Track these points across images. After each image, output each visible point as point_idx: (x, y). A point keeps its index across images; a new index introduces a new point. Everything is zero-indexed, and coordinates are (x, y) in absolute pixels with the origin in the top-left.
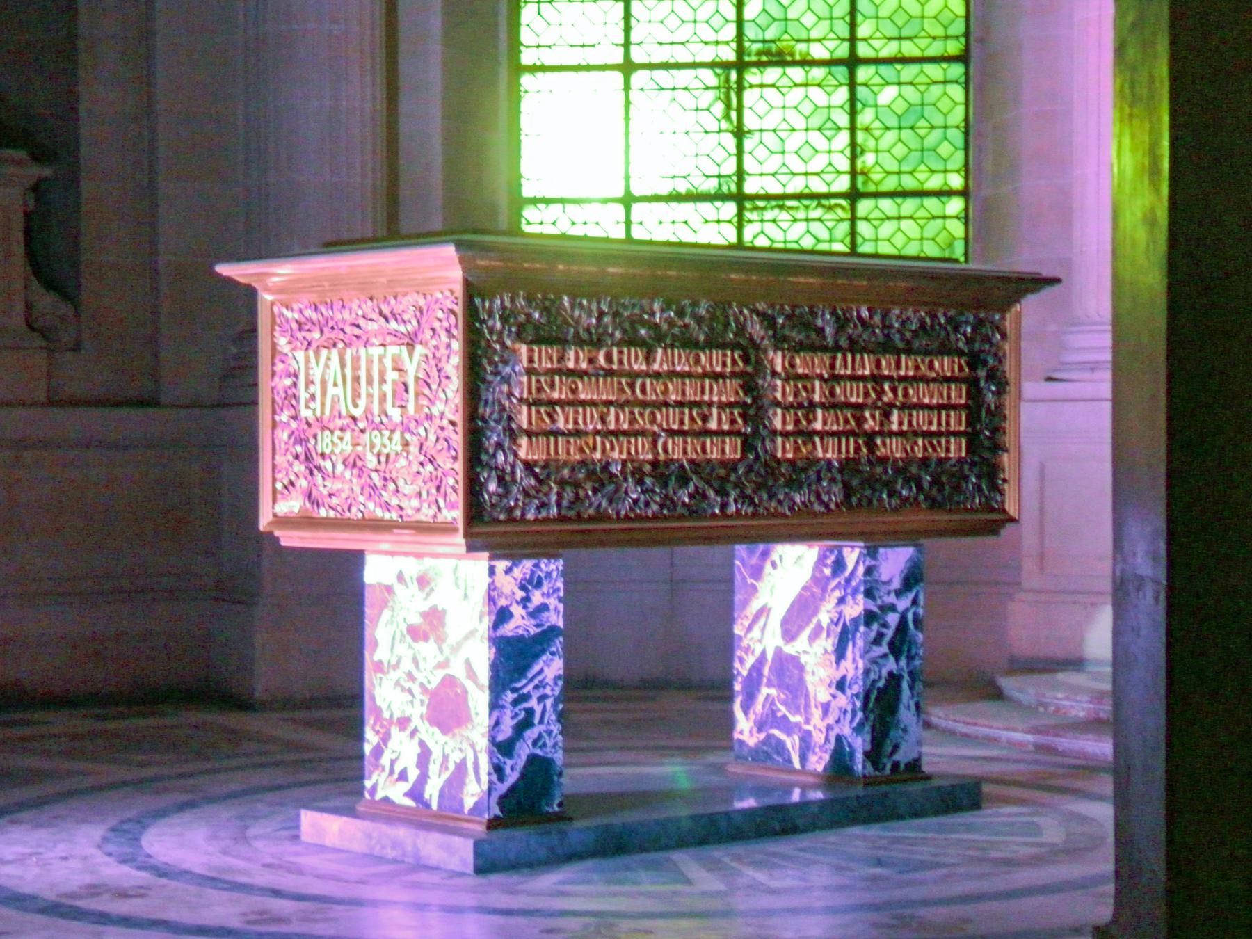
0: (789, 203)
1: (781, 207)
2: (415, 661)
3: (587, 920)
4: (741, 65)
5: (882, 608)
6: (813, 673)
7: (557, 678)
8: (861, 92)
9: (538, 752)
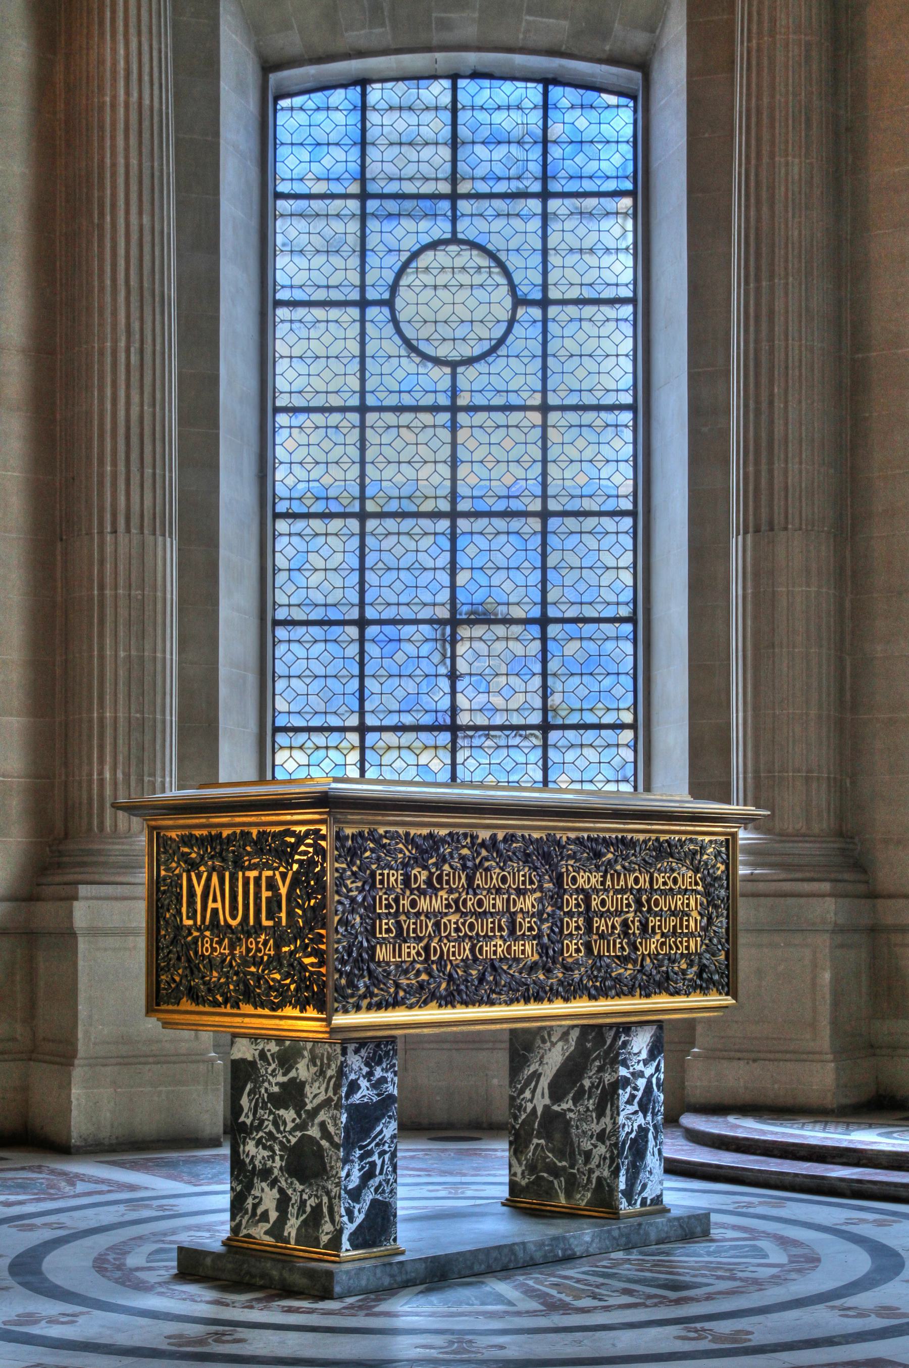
0: (492, 733)
1: (488, 737)
2: (275, 1123)
3: (450, 1337)
4: (454, 622)
5: (633, 1074)
7: (393, 1137)
8: (551, 645)
9: (379, 1197)
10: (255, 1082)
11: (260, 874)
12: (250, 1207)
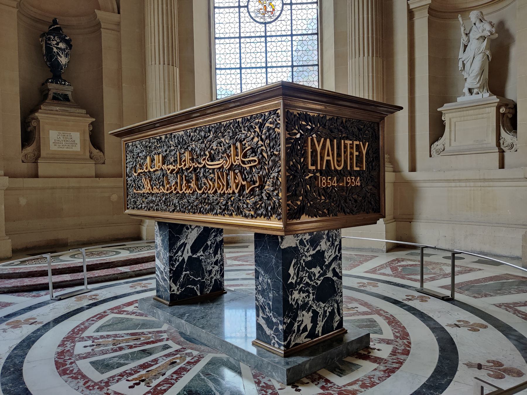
2: (310, 278)
6: (205, 262)
10: (297, 258)
11: (353, 142)
12: (296, 329)
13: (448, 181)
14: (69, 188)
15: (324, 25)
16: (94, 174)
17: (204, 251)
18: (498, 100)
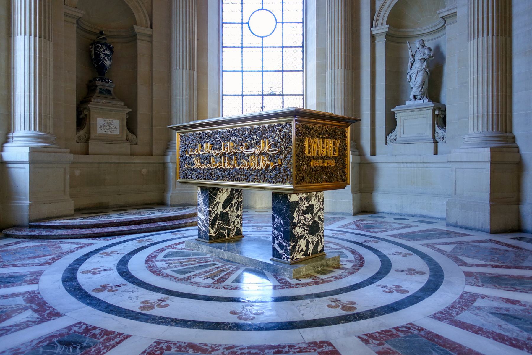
13: (398, 163)
14: (111, 163)
15: (308, 41)
16: (129, 153)
17: (230, 208)
18: (433, 105)
